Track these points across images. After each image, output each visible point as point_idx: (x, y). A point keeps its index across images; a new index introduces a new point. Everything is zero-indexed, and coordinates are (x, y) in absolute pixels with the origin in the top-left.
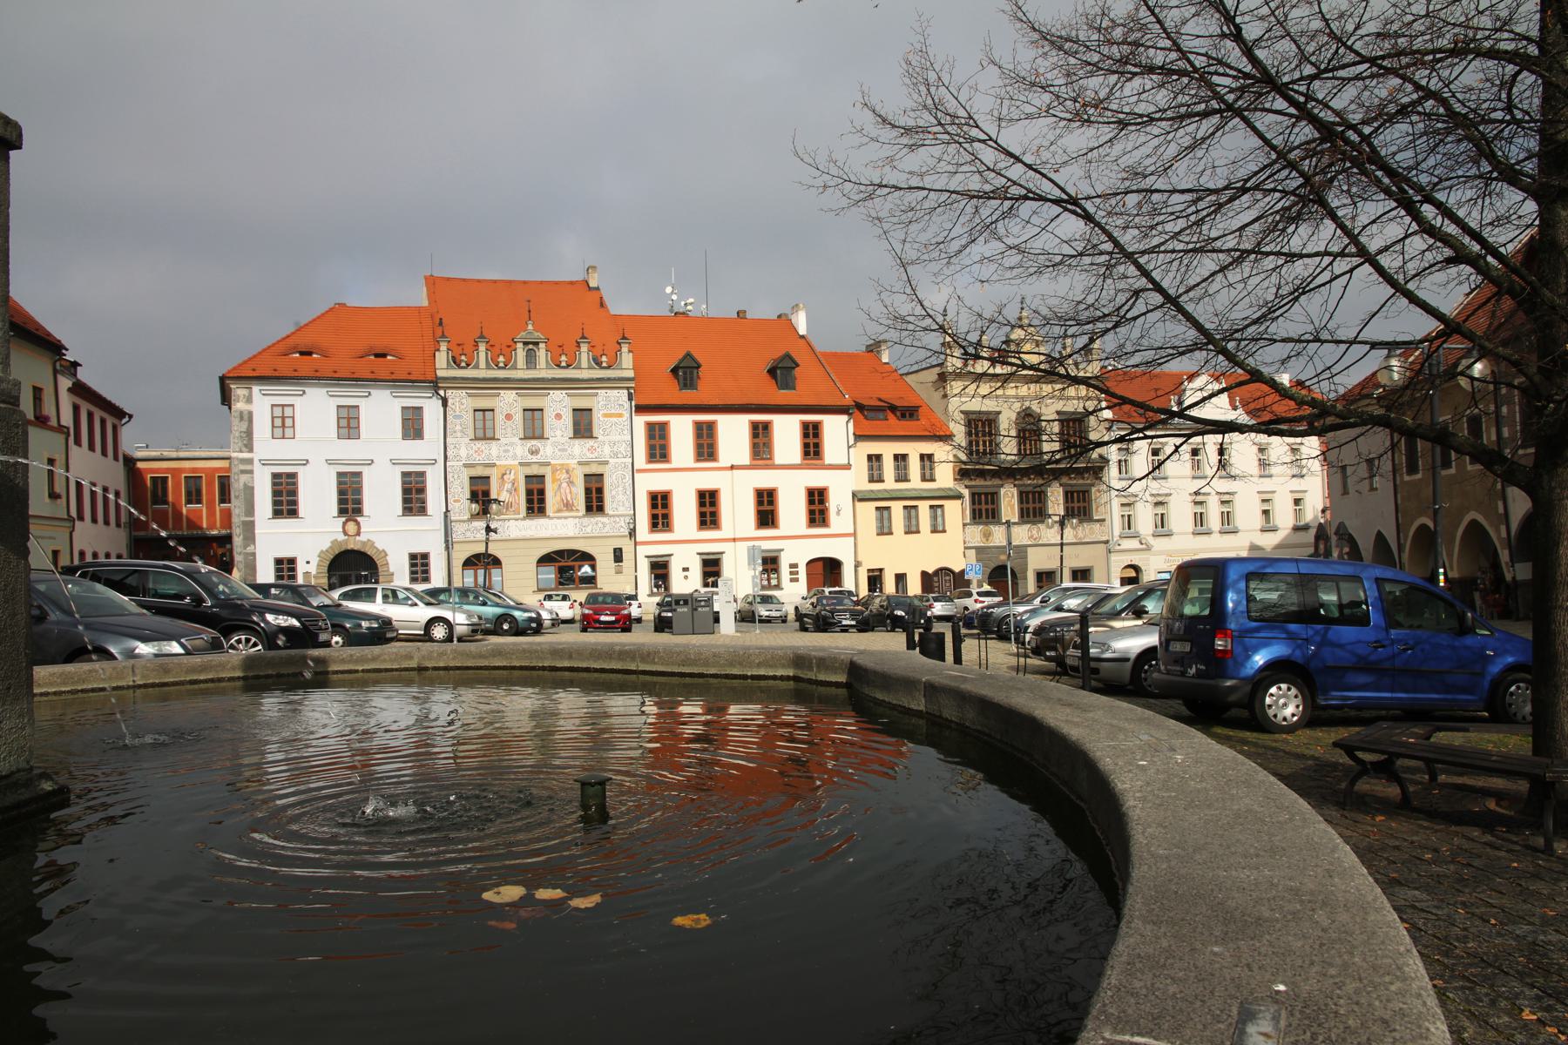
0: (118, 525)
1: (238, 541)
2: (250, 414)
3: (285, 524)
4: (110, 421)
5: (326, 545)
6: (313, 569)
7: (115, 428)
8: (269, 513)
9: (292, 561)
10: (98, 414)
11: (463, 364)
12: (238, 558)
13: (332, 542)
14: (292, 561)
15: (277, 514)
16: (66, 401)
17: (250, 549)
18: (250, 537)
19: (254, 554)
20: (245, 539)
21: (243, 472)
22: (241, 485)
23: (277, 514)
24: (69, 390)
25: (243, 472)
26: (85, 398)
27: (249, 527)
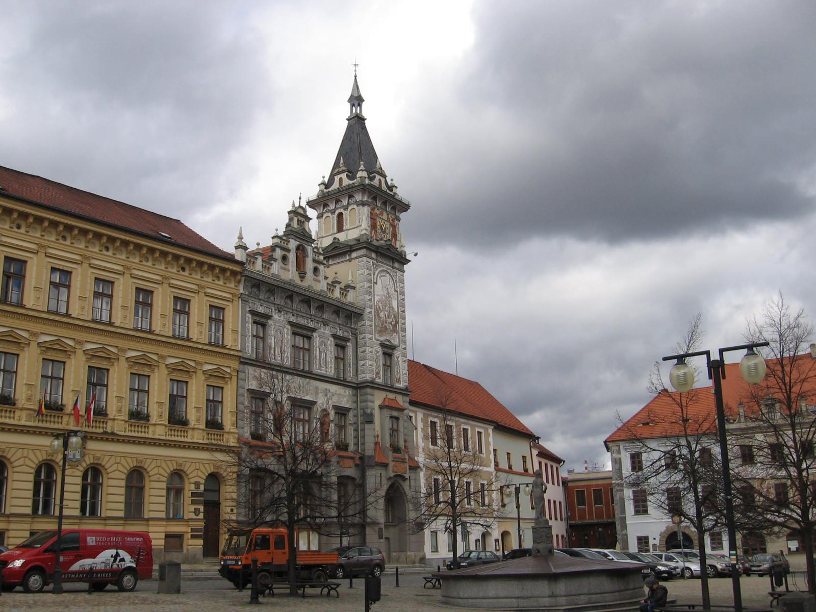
0: (561, 520)
1: (618, 527)
2: (620, 459)
3: (642, 519)
4: (555, 465)
5: (663, 529)
6: (657, 542)
7: (557, 469)
8: (633, 513)
9: (646, 538)
10: (549, 463)
11: (732, 421)
12: (619, 537)
13: (667, 528)
14: (646, 538)
15: (637, 512)
16: (536, 460)
17: (624, 532)
18: (624, 526)
19: (627, 535)
20: (621, 526)
21: (618, 491)
22: (618, 497)
23: (637, 512)
24: (537, 455)
25: (618, 491)
26: (543, 457)
27: (624, 520)
